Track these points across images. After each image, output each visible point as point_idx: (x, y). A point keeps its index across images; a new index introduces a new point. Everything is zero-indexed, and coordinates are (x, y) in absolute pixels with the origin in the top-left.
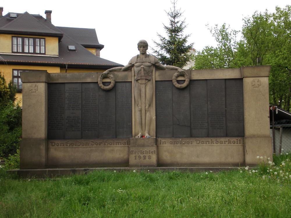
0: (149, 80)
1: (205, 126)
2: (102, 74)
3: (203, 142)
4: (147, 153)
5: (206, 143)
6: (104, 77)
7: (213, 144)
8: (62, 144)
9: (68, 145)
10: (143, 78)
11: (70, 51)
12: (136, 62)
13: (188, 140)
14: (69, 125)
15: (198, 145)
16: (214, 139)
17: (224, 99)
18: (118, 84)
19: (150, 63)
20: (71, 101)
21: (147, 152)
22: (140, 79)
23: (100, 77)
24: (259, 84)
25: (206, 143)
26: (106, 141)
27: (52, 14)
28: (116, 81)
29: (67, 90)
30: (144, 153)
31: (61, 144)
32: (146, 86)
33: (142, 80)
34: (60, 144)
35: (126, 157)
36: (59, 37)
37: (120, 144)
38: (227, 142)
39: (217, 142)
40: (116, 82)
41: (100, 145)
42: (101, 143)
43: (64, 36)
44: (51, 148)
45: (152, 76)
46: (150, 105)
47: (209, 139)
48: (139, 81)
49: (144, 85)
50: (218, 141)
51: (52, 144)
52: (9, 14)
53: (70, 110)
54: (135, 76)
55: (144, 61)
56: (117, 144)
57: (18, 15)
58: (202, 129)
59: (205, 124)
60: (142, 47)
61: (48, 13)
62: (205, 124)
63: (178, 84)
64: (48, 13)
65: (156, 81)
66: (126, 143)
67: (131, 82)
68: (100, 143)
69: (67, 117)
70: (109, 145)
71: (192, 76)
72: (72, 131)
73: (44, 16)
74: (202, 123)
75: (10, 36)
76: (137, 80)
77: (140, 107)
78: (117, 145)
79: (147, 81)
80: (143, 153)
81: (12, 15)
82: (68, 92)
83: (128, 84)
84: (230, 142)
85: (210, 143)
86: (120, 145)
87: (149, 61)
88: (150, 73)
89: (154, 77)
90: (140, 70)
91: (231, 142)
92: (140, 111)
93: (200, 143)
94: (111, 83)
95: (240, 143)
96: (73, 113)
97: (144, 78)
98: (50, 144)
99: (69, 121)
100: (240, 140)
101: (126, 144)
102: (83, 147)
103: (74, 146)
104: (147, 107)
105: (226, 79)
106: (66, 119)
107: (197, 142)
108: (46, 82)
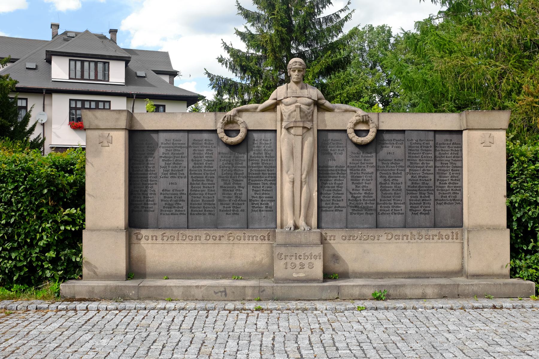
0: (308, 129)
1: (400, 209)
2: (226, 116)
3: (397, 237)
4: (306, 258)
5: (403, 239)
6: (227, 121)
7: (413, 241)
8: (154, 238)
9: (165, 238)
10: (298, 124)
11: (139, 78)
12: (285, 96)
13: (372, 232)
14: (166, 204)
15: (388, 241)
16: (415, 232)
17: (432, 163)
18: (250, 133)
19: (310, 98)
20: (170, 162)
21: (307, 256)
22: (292, 127)
23: (221, 120)
24: (491, 141)
25: (403, 239)
26: (231, 233)
27: (117, 34)
28: (250, 129)
29: (162, 143)
30: (301, 257)
31: (152, 237)
32: (302, 139)
33: (296, 128)
34: (150, 237)
35: (266, 261)
36: (127, 61)
37: (255, 238)
38: (437, 237)
39: (421, 237)
40: (249, 131)
41: (220, 240)
42: (223, 236)
43: (132, 59)
44: (135, 244)
45: (312, 121)
46: (309, 173)
47: (407, 232)
48: (292, 131)
49: (300, 137)
50: (422, 236)
51: (137, 236)
52: (65, 33)
53: (167, 177)
54: (282, 120)
55: (300, 95)
56: (251, 238)
57: (77, 34)
58: (395, 214)
59: (399, 205)
60: (297, 71)
61: (113, 32)
62: (399, 205)
63: (357, 137)
64: (113, 32)
65: (318, 131)
66: (266, 238)
67: (275, 131)
68: (220, 237)
69: (163, 190)
70: (236, 241)
71: (381, 124)
72: (172, 214)
73: (109, 36)
74: (395, 203)
75: (66, 60)
76: (288, 129)
77: (292, 176)
78: (251, 242)
79: (305, 130)
80: (300, 259)
81: (69, 34)
82: (163, 146)
83: (269, 135)
84: (441, 237)
85: (409, 238)
86: (255, 242)
87: (309, 96)
88: (309, 117)
89: (315, 122)
90: (293, 110)
91: (444, 237)
92: (291, 183)
93: (393, 239)
94: (241, 131)
95: (457, 239)
96: (172, 183)
97: (301, 125)
98: (134, 237)
99: (165, 197)
100: (457, 234)
101: (265, 240)
102: (190, 244)
103: (176, 241)
104: (304, 176)
105: (436, 132)
106: (161, 194)
107: (387, 236)
108: (127, 128)
